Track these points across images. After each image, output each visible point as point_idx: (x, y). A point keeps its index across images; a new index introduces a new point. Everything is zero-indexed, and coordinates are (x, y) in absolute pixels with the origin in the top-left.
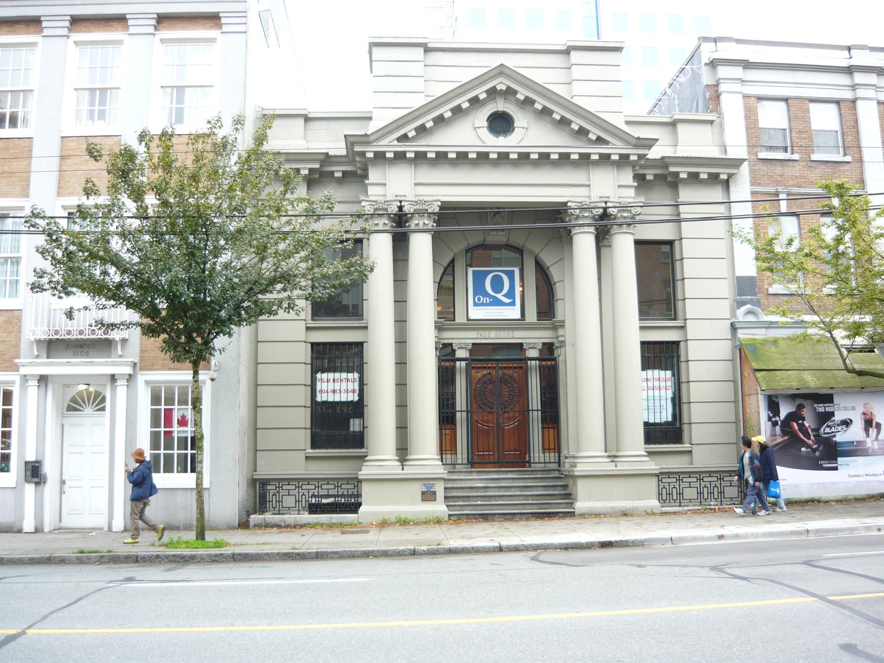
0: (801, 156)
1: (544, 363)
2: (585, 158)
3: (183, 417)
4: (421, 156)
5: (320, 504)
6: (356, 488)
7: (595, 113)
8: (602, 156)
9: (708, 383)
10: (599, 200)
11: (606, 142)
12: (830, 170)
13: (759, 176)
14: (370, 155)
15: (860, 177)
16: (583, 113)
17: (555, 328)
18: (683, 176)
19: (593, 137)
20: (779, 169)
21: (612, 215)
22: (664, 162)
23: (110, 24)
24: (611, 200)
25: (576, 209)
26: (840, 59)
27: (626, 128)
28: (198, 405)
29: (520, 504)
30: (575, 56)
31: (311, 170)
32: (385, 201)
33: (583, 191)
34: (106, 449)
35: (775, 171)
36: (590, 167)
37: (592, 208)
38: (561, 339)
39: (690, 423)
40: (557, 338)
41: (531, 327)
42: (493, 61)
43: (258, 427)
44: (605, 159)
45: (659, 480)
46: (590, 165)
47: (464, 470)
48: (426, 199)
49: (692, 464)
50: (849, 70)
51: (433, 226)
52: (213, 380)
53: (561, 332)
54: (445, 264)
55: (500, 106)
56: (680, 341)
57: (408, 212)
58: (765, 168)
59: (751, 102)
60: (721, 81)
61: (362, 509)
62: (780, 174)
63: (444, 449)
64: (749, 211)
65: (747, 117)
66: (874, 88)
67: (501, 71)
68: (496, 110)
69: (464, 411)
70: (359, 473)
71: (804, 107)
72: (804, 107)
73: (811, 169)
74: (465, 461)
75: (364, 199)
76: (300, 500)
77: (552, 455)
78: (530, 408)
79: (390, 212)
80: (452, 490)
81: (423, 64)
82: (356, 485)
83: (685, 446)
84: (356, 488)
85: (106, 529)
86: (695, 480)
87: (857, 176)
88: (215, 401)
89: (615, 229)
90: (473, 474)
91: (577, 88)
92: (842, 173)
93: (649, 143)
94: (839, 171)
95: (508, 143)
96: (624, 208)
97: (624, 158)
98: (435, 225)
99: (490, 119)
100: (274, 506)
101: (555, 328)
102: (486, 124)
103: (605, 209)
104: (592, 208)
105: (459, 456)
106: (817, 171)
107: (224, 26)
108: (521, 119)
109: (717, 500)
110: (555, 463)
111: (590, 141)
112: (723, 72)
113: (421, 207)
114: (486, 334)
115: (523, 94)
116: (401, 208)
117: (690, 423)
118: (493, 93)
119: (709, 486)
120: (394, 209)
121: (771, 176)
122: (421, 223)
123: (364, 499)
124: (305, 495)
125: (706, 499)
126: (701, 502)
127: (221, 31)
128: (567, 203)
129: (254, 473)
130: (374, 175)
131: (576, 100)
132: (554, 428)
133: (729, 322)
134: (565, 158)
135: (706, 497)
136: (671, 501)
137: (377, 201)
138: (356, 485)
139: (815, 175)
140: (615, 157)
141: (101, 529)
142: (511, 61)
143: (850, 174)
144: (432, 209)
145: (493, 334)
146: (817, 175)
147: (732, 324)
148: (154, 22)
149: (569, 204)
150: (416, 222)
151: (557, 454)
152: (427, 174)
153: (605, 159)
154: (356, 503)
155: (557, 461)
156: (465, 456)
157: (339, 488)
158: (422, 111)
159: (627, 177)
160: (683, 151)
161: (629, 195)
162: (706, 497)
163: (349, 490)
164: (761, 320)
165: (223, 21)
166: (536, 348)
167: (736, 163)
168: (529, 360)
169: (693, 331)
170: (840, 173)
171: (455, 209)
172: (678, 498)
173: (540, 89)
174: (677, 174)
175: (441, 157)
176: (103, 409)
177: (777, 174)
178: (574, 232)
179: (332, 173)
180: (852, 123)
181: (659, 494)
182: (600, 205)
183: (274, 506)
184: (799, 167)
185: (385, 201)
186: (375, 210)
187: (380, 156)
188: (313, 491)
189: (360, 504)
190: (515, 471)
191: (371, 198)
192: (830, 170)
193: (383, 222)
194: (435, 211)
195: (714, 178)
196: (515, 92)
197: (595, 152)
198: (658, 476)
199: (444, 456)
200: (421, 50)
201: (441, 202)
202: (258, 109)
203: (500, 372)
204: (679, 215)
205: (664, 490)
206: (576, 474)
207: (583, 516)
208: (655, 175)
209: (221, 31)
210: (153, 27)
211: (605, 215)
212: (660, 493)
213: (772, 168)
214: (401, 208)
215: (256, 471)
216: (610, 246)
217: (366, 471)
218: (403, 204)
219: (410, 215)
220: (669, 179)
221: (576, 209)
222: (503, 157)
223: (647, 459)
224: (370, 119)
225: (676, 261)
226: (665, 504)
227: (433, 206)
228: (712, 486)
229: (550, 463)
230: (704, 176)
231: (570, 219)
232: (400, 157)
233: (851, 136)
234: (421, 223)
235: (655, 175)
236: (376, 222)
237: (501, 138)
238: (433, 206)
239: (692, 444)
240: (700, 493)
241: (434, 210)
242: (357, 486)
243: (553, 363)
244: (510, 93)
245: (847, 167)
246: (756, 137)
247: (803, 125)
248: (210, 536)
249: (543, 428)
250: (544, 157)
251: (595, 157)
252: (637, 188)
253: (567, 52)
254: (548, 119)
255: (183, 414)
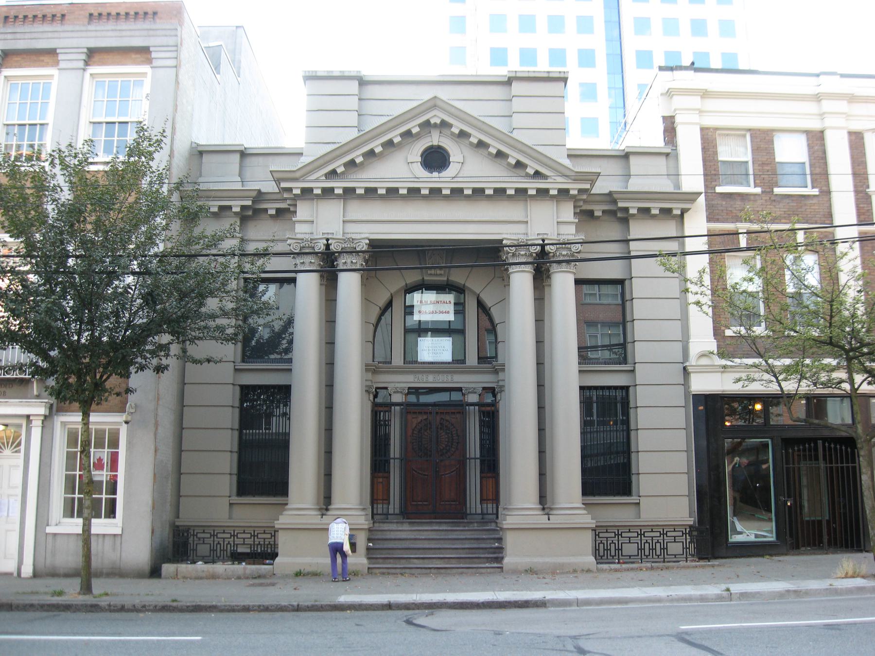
0: (764, 190)
1: (483, 409)
2: (521, 193)
3: (100, 460)
4: (349, 192)
5: (235, 553)
6: (273, 538)
7: (532, 146)
8: (539, 191)
9: (672, 430)
10: (537, 237)
11: (545, 177)
12: (795, 204)
13: (717, 211)
14: (297, 192)
15: (828, 211)
16: (520, 146)
17: (496, 372)
18: (633, 211)
19: (531, 171)
20: (739, 203)
21: (550, 253)
22: (611, 198)
23: (42, 58)
24: (549, 237)
25: (512, 246)
26: (808, 86)
27: (567, 162)
28: (87, 448)
29: (469, 558)
30: (517, 88)
31: (243, 208)
32: (311, 239)
33: (521, 228)
34: (19, 491)
35: (735, 206)
36: (529, 201)
37: (529, 245)
38: (501, 383)
39: (639, 474)
40: (498, 382)
41: (472, 371)
42: (426, 94)
43: (182, 472)
44: (543, 193)
45: (596, 535)
46: (528, 199)
47: (395, 521)
48: (354, 236)
49: (640, 518)
50: (818, 98)
51: (362, 265)
52: (127, 422)
53: (501, 375)
54: (382, 301)
55: (435, 139)
56: (630, 386)
57: (335, 250)
58: (724, 203)
59: (710, 134)
60: (677, 112)
61: (277, 560)
62: (740, 209)
63: (375, 498)
64: (705, 248)
65: (704, 149)
66: (844, 116)
67: (434, 104)
68: (430, 144)
69: (397, 458)
70: (275, 522)
71: (767, 138)
72: (767, 138)
73: (774, 203)
74: (397, 511)
75: (290, 237)
76: (222, 552)
77: (490, 506)
78: (468, 456)
79: (317, 251)
80: (379, 542)
81: (356, 98)
82: (273, 534)
83: (633, 499)
84: (273, 538)
85: (15, 574)
86: (636, 534)
87: (825, 210)
88: (130, 443)
89: (554, 268)
90: (405, 524)
91: (518, 121)
92: (808, 207)
93: (592, 178)
94: (805, 205)
95: (444, 179)
96: (564, 246)
97: (564, 193)
98: (364, 264)
99: (424, 156)
100: (218, 555)
101: (496, 372)
102: (420, 159)
103: (543, 246)
104: (529, 245)
105: (391, 506)
106: (781, 205)
107: (154, 60)
108: (456, 153)
109: (614, 557)
110: (493, 514)
111: (528, 175)
112: (679, 102)
113: (349, 245)
114: (424, 377)
115: (457, 127)
116: (328, 246)
117: (639, 474)
118: (427, 125)
119: (222, 543)
120: (320, 247)
121: (731, 211)
122: (349, 261)
123: (280, 551)
124: (220, 544)
125: (647, 556)
126: (664, 558)
127: (152, 66)
128: (502, 240)
129: (176, 520)
130: (303, 211)
131: (516, 135)
132: (494, 477)
133: (681, 366)
134: (500, 193)
135: (647, 553)
136: (609, 557)
137: (303, 239)
138: (273, 534)
139: (778, 210)
140: (553, 192)
141: (11, 574)
142: (444, 94)
143: (817, 208)
144: (360, 247)
145: (431, 378)
146: (781, 210)
147: (685, 368)
148: (84, 57)
149: (504, 242)
150: (344, 261)
151: (495, 505)
152: (359, 210)
153: (543, 193)
154: (273, 554)
155: (495, 512)
156: (397, 505)
157: (256, 538)
158: (352, 145)
159: (568, 212)
160: (635, 185)
161: (569, 232)
162: (647, 553)
163: (266, 540)
164: (716, 364)
165: (154, 55)
166: (475, 393)
167: (692, 197)
168: (467, 405)
169: (642, 374)
170: (806, 207)
171: (393, 247)
172: (222, 556)
173: (475, 122)
174: (626, 210)
175: (370, 192)
176: (18, 451)
177: (737, 209)
178: (511, 270)
179: (266, 210)
180: (820, 154)
181: (596, 550)
182: (537, 242)
183: (218, 555)
184: (761, 201)
185: (311, 239)
186: (301, 248)
187: (307, 192)
188: (269, 540)
189: (276, 555)
190: (449, 523)
191: (298, 236)
192: (795, 204)
193: (312, 262)
194: (363, 249)
195: (666, 212)
196: (450, 126)
197: (532, 186)
198: (595, 530)
199: (375, 506)
200: (356, 83)
201: (369, 240)
202: (194, 145)
203: (438, 418)
204: (629, 252)
205: (601, 545)
206: (505, 527)
207: (516, 572)
208: (604, 212)
209: (152, 66)
210: (83, 61)
211: (543, 253)
212: (597, 548)
213: (732, 203)
214: (328, 246)
215: (178, 517)
216: (550, 285)
217: (284, 520)
218: (329, 242)
219: (336, 254)
220: (619, 215)
221: (512, 246)
222: (435, 193)
223: (585, 512)
224: (302, 154)
225: (627, 301)
226: (601, 561)
227: (361, 244)
228: (654, 542)
229: (476, 514)
230: (655, 212)
231: (507, 258)
232: (328, 192)
233: (819, 167)
234: (349, 261)
235: (604, 212)
236: (302, 261)
237: (435, 174)
238: (361, 244)
239: (640, 496)
240: (641, 549)
241: (363, 248)
242: (275, 536)
243: (493, 408)
244: (444, 124)
245: (815, 201)
246: (715, 170)
247: (766, 157)
248: (98, 586)
249: (481, 478)
250: (478, 193)
251: (532, 192)
252: (577, 225)
253: (509, 82)
254: (485, 152)
255: (100, 457)
